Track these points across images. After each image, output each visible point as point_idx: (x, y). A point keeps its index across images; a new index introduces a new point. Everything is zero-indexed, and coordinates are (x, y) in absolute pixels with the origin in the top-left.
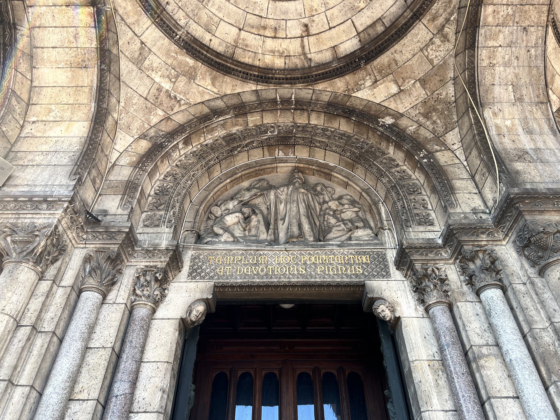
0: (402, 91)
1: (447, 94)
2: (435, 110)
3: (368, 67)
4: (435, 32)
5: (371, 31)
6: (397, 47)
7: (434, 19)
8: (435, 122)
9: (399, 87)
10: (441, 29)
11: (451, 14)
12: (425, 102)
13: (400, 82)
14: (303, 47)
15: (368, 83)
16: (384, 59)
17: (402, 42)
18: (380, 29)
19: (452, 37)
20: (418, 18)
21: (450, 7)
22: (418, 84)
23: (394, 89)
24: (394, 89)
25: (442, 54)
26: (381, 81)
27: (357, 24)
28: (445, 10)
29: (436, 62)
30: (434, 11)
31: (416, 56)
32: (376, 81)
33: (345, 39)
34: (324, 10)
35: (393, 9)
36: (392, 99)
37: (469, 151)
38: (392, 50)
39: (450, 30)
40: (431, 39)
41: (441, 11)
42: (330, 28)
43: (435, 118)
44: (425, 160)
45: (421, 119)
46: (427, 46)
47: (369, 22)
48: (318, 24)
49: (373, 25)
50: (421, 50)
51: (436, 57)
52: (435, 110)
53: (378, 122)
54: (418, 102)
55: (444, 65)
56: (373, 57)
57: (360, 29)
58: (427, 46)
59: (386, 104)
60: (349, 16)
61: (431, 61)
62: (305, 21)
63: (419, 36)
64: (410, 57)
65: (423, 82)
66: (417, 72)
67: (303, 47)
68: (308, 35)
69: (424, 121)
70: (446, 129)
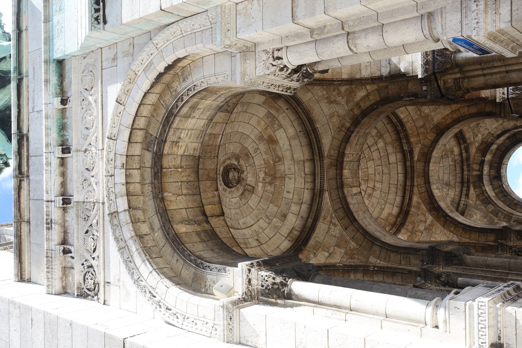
0: (330, 253)
1: (353, 246)
2: (353, 254)
3: (307, 248)
4: (329, 224)
5: (291, 235)
6: (315, 235)
7: (325, 219)
8: (358, 259)
9: (328, 252)
10: (331, 222)
11: (332, 214)
12: (346, 254)
13: (327, 250)
14: (263, 250)
15: (312, 256)
16: (312, 242)
17: (316, 232)
18: (296, 233)
19: (337, 223)
20: (317, 221)
21: (330, 211)
22: (336, 248)
23: (327, 254)
24: (327, 254)
25: (338, 231)
26: (317, 253)
27: (283, 234)
28: (328, 214)
29: (337, 236)
30: (323, 216)
31: (326, 236)
32: (315, 254)
33: (281, 242)
34: (262, 231)
35: (298, 222)
36: (329, 258)
37: (388, 257)
38: (313, 237)
39: (335, 221)
40: (329, 227)
41: (327, 215)
42: (270, 239)
43: (357, 257)
44: (376, 268)
45: (350, 260)
46: (329, 230)
47: (288, 231)
48: (263, 239)
49: (291, 232)
50: (327, 233)
51: (336, 233)
52: (353, 254)
53: (337, 266)
54: (342, 255)
55: (342, 236)
56: (305, 243)
57: (286, 236)
58: (329, 230)
59: (327, 262)
60: (276, 231)
61: (335, 236)
62: (256, 237)
63: (322, 228)
64: (323, 238)
65: (338, 245)
66: (331, 243)
67: (263, 250)
68: (262, 244)
69: (352, 261)
70: (366, 258)
